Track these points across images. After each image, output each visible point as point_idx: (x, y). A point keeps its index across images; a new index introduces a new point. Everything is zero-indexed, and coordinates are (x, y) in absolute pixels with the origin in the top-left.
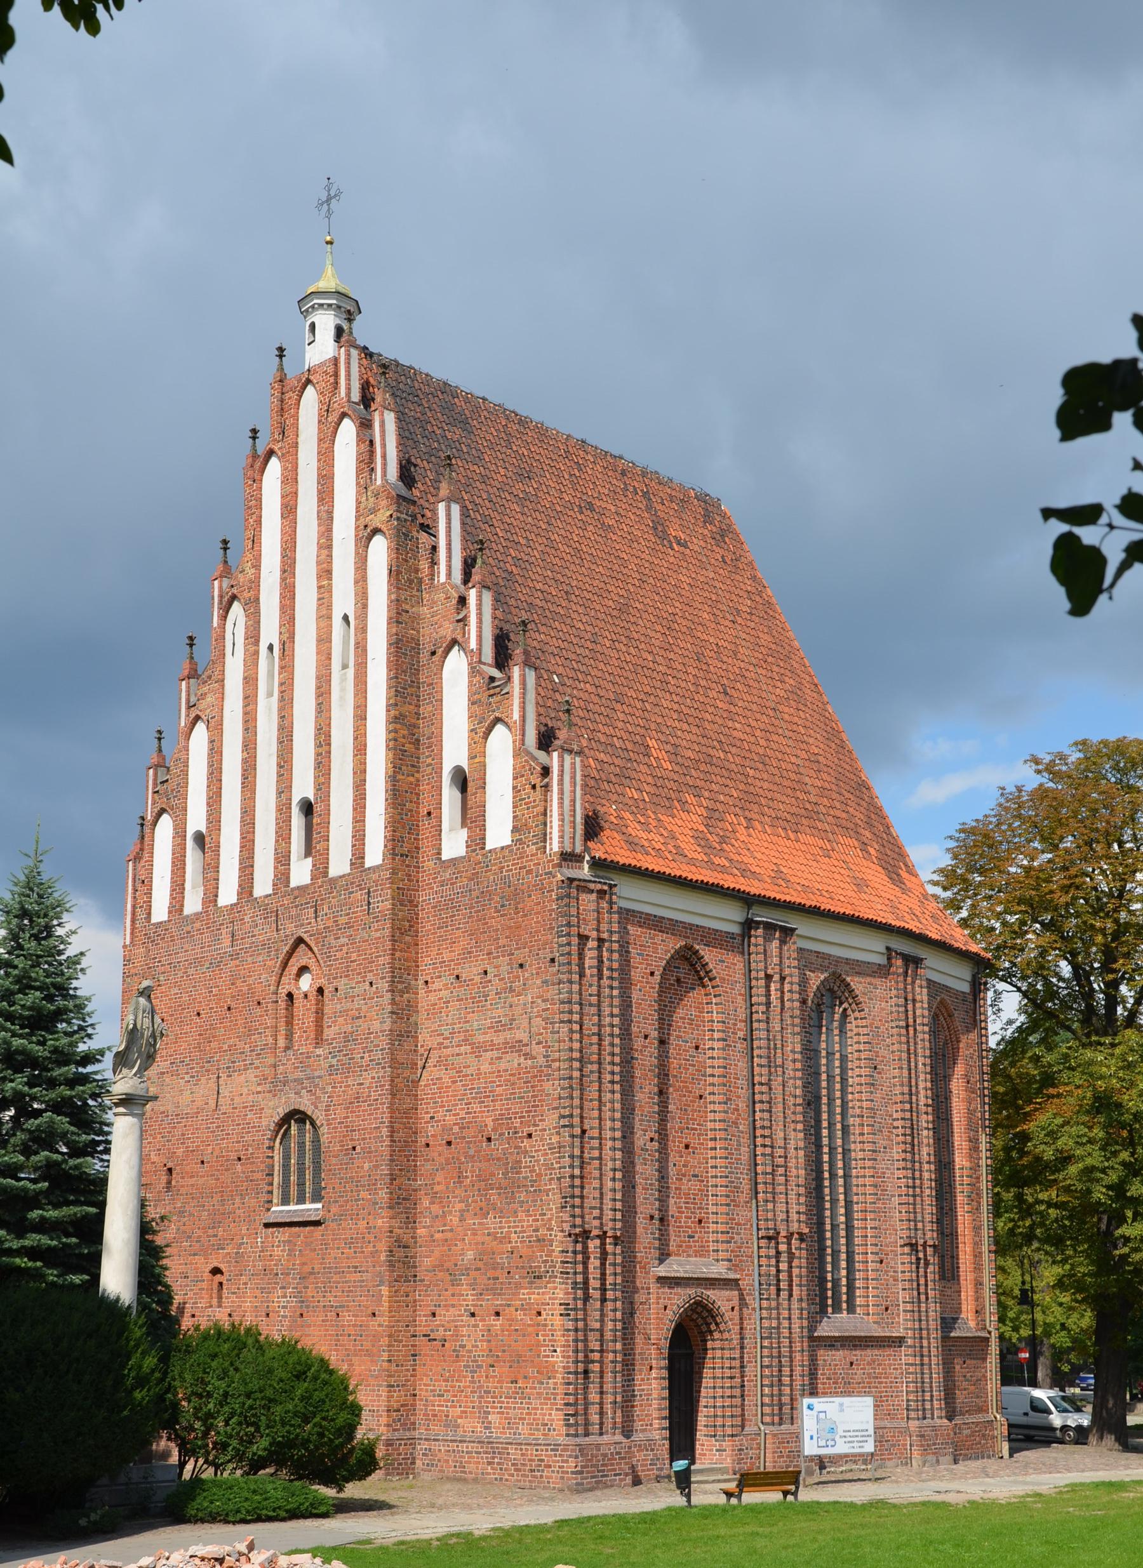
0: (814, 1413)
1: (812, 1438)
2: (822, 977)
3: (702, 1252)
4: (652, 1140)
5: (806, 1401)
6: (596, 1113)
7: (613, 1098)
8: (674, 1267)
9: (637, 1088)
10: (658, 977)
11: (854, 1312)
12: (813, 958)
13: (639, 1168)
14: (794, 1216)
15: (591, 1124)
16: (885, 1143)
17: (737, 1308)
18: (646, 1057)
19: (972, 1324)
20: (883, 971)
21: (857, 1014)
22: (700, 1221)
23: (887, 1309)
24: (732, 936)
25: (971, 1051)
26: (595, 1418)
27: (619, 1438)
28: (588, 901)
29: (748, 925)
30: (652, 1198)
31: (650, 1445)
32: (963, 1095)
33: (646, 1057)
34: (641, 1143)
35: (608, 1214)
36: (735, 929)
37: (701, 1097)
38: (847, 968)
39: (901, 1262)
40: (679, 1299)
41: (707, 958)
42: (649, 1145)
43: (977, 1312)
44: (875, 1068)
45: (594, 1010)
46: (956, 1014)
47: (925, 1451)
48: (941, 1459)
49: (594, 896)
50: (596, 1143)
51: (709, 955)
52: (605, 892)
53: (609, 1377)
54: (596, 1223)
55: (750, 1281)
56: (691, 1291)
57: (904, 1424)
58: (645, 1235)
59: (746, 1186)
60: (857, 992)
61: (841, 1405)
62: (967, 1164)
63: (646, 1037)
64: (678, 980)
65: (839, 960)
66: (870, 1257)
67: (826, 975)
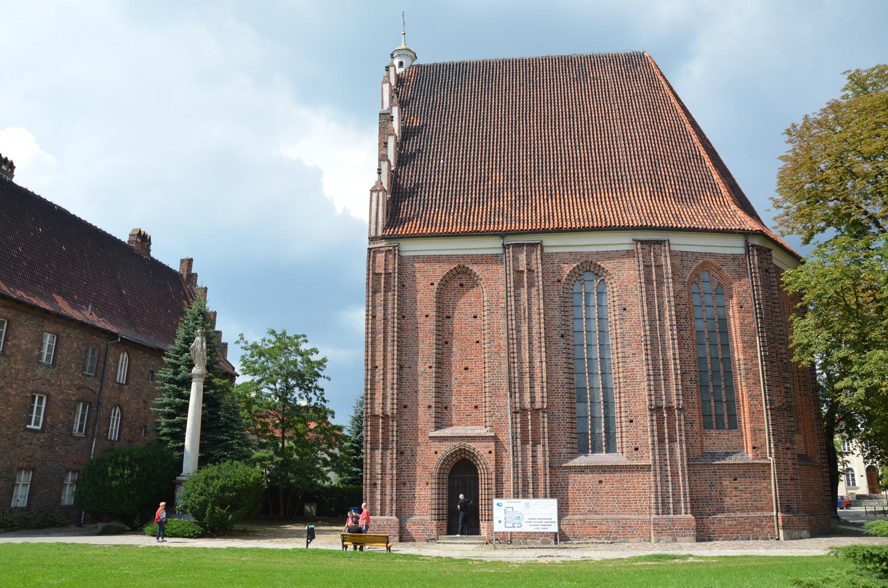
0: (503, 508)
1: (500, 522)
2: (575, 265)
3: (476, 423)
4: (430, 367)
5: (496, 501)
6: (382, 358)
7: (393, 349)
8: (447, 432)
9: (420, 342)
10: (436, 285)
11: (615, 452)
12: (567, 256)
13: (420, 382)
14: (538, 399)
15: (379, 363)
16: (634, 352)
17: (493, 452)
18: (426, 328)
19: (750, 456)
20: (629, 254)
21: (613, 281)
22: (476, 407)
23: (636, 449)
24: (497, 255)
25: (745, 288)
26: (379, 507)
27: (394, 518)
28: (380, 257)
29: (505, 247)
30: (430, 397)
31: (422, 523)
32: (737, 315)
33: (426, 328)
34: (422, 369)
35: (389, 406)
36: (501, 251)
37: (478, 342)
38: (598, 257)
39: (646, 421)
40: (446, 448)
41: (475, 270)
42: (428, 370)
43: (754, 448)
44: (625, 309)
45: (382, 308)
46: (724, 268)
47: (659, 533)
48: (678, 539)
49: (384, 254)
50: (381, 372)
51: (475, 268)
52: (390, 250)
53: (388, 487)
54: (381, 411)
55: (506, 437)
56: (457, 444)
57: (648, 517)
58: (425, 416)
59: (505, 385)
60: (607, 269)
61: (527, 504)
62: (741, 357)
63: (427, 316)
64: (461, 285)
65: (589, 254)
66: (623, 419)
67: (578, 263)
